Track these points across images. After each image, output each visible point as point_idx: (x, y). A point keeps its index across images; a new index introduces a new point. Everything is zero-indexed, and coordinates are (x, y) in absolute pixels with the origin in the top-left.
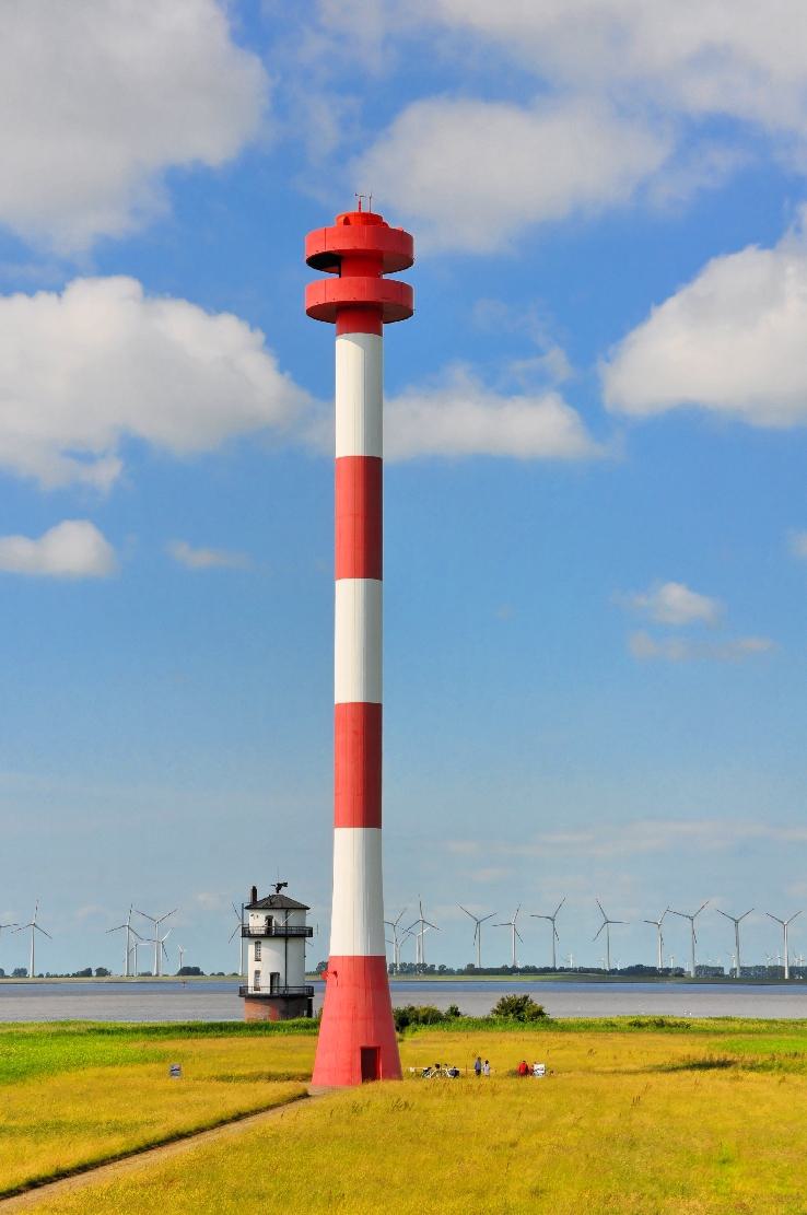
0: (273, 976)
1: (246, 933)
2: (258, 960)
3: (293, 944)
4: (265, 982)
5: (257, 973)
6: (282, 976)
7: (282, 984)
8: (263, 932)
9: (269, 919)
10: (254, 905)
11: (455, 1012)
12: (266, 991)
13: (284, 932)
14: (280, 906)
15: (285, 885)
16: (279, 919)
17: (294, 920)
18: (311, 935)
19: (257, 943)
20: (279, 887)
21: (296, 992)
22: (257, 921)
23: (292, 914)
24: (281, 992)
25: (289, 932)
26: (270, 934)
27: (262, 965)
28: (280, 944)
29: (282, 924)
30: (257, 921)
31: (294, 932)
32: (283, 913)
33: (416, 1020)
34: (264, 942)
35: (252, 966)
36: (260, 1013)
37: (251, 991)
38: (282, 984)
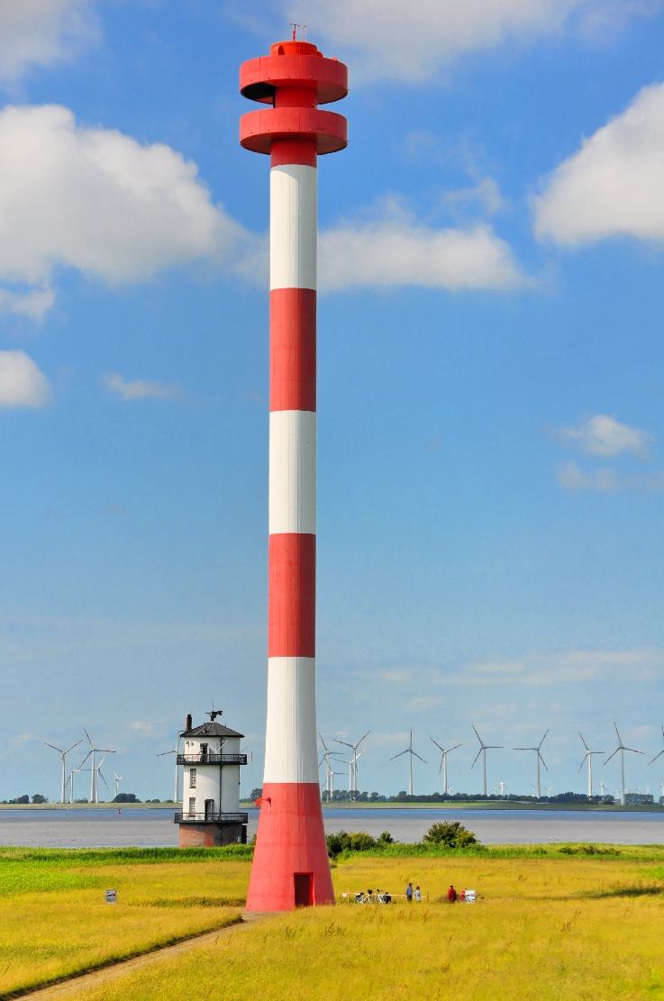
0: (208, 803)
1: (181, 761)
3: (227, 771)
4: (200, 808)
5: (192, 800)
6: (217, 803)
8: (197, 759)
9: (204, 747)
15: (220, 713)
16: (213, 746)
17: (228, 748)
19: (192, 771)
20: (214, 715)
22: (192, 749)
23: (226, 742)
26: (205, 761)
28: (214, 771)
30: (192, 749)
33: (349, 846)
34: (199, 769)
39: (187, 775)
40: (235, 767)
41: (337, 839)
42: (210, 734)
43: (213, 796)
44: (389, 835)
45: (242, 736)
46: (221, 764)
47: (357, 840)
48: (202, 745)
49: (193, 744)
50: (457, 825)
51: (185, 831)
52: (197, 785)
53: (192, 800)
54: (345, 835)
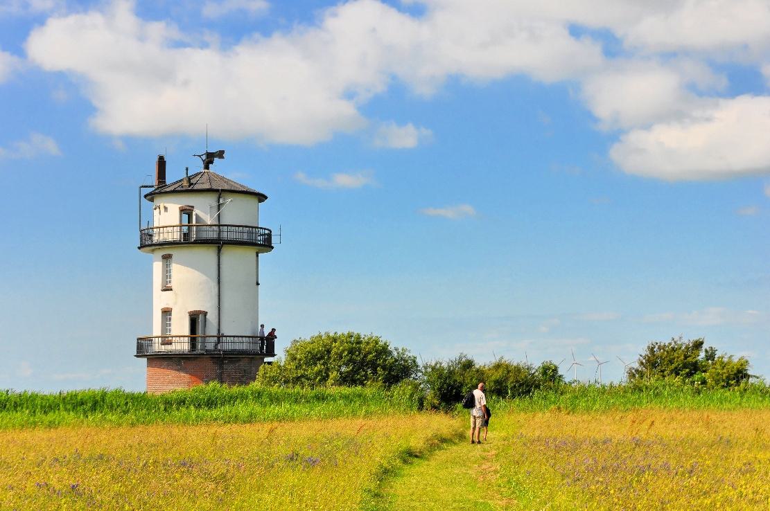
1: (147, 242)
2: (167, 289)
3: (232, 256)
4: (180, 326)
5: (167, 313)
6: (212, 318)
7: (212, 330)
8: (175, 235)
9: (187, 211)
10: (161, 189)
11: (550, 374)
12: (183, 346)
13: (212, 234)
14: (207, 186)
15: (220, 154)
16: (204, 210)
17: (236, 212)
18: (267, 245)
19: (167, 258)
20: (210, 158)
21: (237, 347)
22: (167, 217)
23: (229, 200)
24: (210, 346)
25: (224, 235)
27: (179, 293)
28: (209, 254)
29: (209, 219)
30: (167, 217)
31: (232, 236)
32: (211, 200)
34: (176, 253)
35: (161, 300)
36: (175, 383)
37: (158, 347)
38: (212, 330)
39: (158, 266)
40: (249, 253)
41: (451, 373)
42: (196, 187)
43: (204, 303)
44: (555, 370)
45: (261, 197)
46: (219, 244)
47: (497, 375)
48: (183, 211)
49: (166, 209)
50: (706, 351)
51: (157, 370)
52: (173, 285)
53: (167, 313)
54: (469, 365)
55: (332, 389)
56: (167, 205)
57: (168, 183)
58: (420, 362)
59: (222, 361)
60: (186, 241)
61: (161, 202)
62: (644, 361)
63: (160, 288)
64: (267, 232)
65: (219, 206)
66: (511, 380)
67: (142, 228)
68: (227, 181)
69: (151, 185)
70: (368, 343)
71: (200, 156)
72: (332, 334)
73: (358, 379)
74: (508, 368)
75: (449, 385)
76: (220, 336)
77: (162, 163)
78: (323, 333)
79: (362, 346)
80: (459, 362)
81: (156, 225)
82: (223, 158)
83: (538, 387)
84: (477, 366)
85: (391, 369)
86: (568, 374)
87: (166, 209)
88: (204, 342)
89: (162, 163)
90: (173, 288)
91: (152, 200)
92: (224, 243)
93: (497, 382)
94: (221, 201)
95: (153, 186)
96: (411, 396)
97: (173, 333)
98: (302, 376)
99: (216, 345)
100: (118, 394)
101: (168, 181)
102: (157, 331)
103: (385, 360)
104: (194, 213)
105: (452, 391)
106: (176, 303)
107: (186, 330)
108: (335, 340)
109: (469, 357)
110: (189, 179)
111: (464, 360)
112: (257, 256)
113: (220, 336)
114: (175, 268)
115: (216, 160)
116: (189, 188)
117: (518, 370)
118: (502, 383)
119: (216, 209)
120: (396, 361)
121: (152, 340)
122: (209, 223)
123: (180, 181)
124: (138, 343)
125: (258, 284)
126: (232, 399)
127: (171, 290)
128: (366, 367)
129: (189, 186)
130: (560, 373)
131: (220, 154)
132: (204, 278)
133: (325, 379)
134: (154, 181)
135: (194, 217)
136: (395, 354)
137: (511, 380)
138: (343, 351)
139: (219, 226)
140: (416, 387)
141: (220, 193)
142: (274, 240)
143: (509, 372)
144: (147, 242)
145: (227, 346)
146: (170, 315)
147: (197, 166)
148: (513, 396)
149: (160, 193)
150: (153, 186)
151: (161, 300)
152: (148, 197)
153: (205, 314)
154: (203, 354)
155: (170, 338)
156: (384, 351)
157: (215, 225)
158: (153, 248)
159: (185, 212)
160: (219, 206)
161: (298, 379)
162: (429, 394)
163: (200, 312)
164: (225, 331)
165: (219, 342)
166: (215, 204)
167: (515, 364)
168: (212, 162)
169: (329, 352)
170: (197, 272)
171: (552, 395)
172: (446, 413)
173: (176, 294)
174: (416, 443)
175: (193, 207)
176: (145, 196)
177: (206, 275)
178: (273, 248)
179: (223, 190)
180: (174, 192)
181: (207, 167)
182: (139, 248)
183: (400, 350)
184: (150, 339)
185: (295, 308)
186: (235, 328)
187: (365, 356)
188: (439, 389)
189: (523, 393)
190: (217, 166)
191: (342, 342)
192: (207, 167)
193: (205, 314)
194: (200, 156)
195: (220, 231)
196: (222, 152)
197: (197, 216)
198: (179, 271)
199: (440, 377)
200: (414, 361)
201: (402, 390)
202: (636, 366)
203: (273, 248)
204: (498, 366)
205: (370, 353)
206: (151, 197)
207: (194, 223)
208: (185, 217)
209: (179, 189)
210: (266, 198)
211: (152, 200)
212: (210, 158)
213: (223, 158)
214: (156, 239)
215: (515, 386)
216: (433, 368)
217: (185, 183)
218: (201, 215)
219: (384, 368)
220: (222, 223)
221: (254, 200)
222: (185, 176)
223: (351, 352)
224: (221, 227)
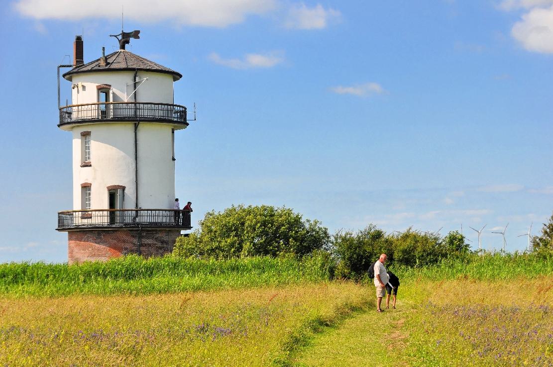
0: (113, 194)
1: (65, 119)
2: (86, 165)
4: (100, 201)
5: (86, 187)
6: (130, 192)
7: (130, 205)
8: (93, 113)
9: (104, 90)
10: (79, 68)
11: (457, 243)
12: (101, 219)
13: (130, 113)
14: (123, 66)
16: (121, 89)
17: (152, 90)
19: (85, 135)
20: (125, 39)
22: (85, 95)
23: (144, 78)
24: (128, 220)
25: (140, 113)
26: (108, 116)
27: (99, 169)
28: (125, 131)
29: (125, 97)
30: (85, 95)
32: (128, 78)
34: (94, 129)
35: (80, 176)
36: (98, 255)
37: (78, 221)
38: (130, 205)
39: (77, 143)
40: (166, 129)
41: (360, 244)
42: (113, 66)
43: (124, 179)
44: (461, 240)
45: (176, 76)
46: (136, 121)
49: (84, 87)
53: (86, 187)
54: (378, 235)
55: (246, 260)
56: (84, 84)
57: (85, 62)
58: (331, 232)
59: (140, 234)
60: (103, 119)
61: (79, 81)
62: (548, 230)
63: (80, 164)
64: (181, 109)
65: (135, 85)
66: (419, 249)
67: (62, 106)
68: (142, 60)
69: (69, 64)
70: (281, 216)
71: (116, 36)
72: (246, 207)
73: (271, 250)
74: (415, 238)
75: (358, 255)
76: (138, 210)
77: (79, 43)
78: (236, 206)
79: (275, 218)
80: (368, 233)
81: (74, 103)
82: (139, 38)
83: (445, 256)
84: (386, 236)
85: (302, 240)
86: (474, 243)
87: (84, 87)
88: (123, 216)
89: (79, 43)
90: (92, 164)
91: (70, 79)
92: (140, 121)
93: (405, 252)
94: (137, 80)
95: (70, 66)
96: (323, 265)
97: (92, 208)
98: (219, 248)
99: (135, 218)
100: (37, 267)
101: (86, 60)
102: (77, 205)
103: (297, 232)
104: (111, 92)
105: (358, 259)
106: (95, 179)
107: (106, 205)
108: (249, 213)
109: (378, 228)
110: (106, 59)
111: (373, 230)
112: (173, 132)
113: (138, 210)
114: (94, 145)
115: (132, 40)
116: (106, 67)
117: (425, 239)
118: (410, 253)
119: (133, 88)
120: (308, 232)
121: (72, 214)
122: (126, 101)
123: (99, 60)
124: (59, 217)
125: (174, 159)
126: (150, 272)
127: (90, 166)
128: (280, 238)
129: (106, 65)
130: (466, 242)
131: (136, 34)
132: (122, 154)
133: (240, 249)
134: (73, 61)
135: (111, 96)
136: (307, 226)
137: (419, 249)
138: (256, 224)
139: (135, 104)
140: (326, 257)
141: (135, 71)
142: (189, 116)
143: (417, 242)
144: (65, 119)
145: (145, 218)
146: (90, 190)
147: (113, 46)
148: (421, 265)
149: (77, 73)
150: (70, 66)
151: (80, 176)
152: (67, 76)
153: (123, 188)
154: (122, 227)
155: (90, 213)
156: (297, 222)
157: (132, 103)
158: (74, 125)
159: (104, 90)
160: (135, 85)
161: (213, 250)
162: (340, 263)
163: (119, 187)
164: (142, 205)
165: (137, 216)
166: (132, 83)
167: (423, 234)
168: (128, 42)
169: (243, 224)
170: (114, 148)
171: (458, 265)
172: (357, 281)
173: (95, 170)
174: (327, 311)
175: (110, 86)
176: (64, 76)
177: (125, 153)
178: (188, 124)
179: (138, 69)
180: (92, 71)
181: (123, 47)
182: (59, 126)
183: (312, 222)
184: (70, 214)
185: (209, 183)
186: (152, 202)
187: (279, 228)
188: (350, 259)
189: (430, 262)
190: (133, 46)
191: (255, 216)
192: (123, 47)
193: (123, 188)
194: (116, 36)
195: (136, 109)
196: (138, 32)
197: (113, 93)
198: (97, 147)
199: (350, 248)
200: (325, 233)
201: (314, 261)
202: (540, 235)
203: (188, 124)
204: (406, 237)
205: (283, 225)
206: (69, 76)
207: (111, 100)
208: (103, 95)
209: (96, 68)
210: (181, 76)
211: (70, 79)
212: (125, 39)
213: (139, 38)
214: (74, 116)
215: (423, 256)
216: (344, 239)
217: (102, 63)
218: (118, 93)
219: (295, 239)
220: (140, 100)
221: (168, 79)
222: (102, 56)
223: (264, 224)
224: (138, 105)
